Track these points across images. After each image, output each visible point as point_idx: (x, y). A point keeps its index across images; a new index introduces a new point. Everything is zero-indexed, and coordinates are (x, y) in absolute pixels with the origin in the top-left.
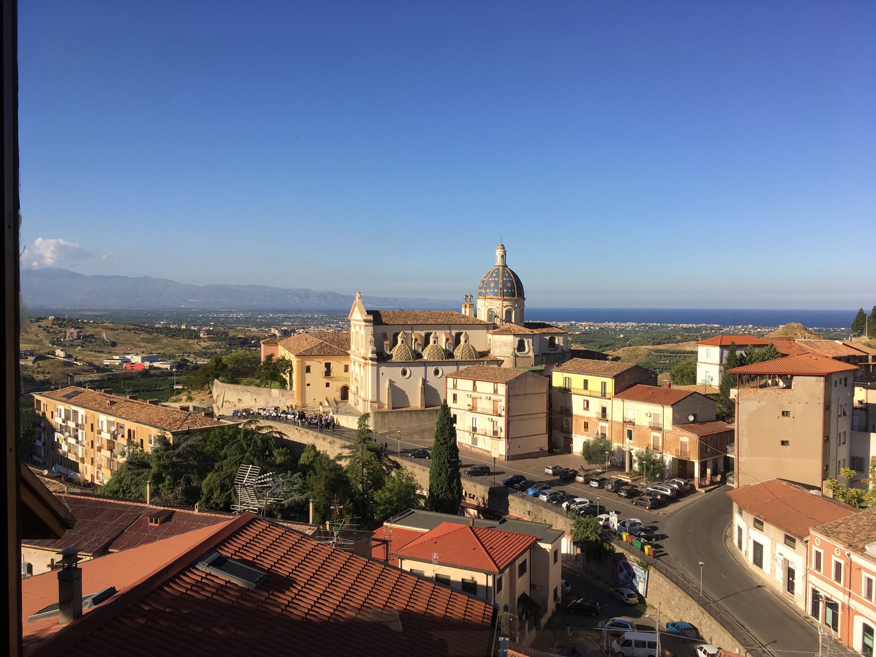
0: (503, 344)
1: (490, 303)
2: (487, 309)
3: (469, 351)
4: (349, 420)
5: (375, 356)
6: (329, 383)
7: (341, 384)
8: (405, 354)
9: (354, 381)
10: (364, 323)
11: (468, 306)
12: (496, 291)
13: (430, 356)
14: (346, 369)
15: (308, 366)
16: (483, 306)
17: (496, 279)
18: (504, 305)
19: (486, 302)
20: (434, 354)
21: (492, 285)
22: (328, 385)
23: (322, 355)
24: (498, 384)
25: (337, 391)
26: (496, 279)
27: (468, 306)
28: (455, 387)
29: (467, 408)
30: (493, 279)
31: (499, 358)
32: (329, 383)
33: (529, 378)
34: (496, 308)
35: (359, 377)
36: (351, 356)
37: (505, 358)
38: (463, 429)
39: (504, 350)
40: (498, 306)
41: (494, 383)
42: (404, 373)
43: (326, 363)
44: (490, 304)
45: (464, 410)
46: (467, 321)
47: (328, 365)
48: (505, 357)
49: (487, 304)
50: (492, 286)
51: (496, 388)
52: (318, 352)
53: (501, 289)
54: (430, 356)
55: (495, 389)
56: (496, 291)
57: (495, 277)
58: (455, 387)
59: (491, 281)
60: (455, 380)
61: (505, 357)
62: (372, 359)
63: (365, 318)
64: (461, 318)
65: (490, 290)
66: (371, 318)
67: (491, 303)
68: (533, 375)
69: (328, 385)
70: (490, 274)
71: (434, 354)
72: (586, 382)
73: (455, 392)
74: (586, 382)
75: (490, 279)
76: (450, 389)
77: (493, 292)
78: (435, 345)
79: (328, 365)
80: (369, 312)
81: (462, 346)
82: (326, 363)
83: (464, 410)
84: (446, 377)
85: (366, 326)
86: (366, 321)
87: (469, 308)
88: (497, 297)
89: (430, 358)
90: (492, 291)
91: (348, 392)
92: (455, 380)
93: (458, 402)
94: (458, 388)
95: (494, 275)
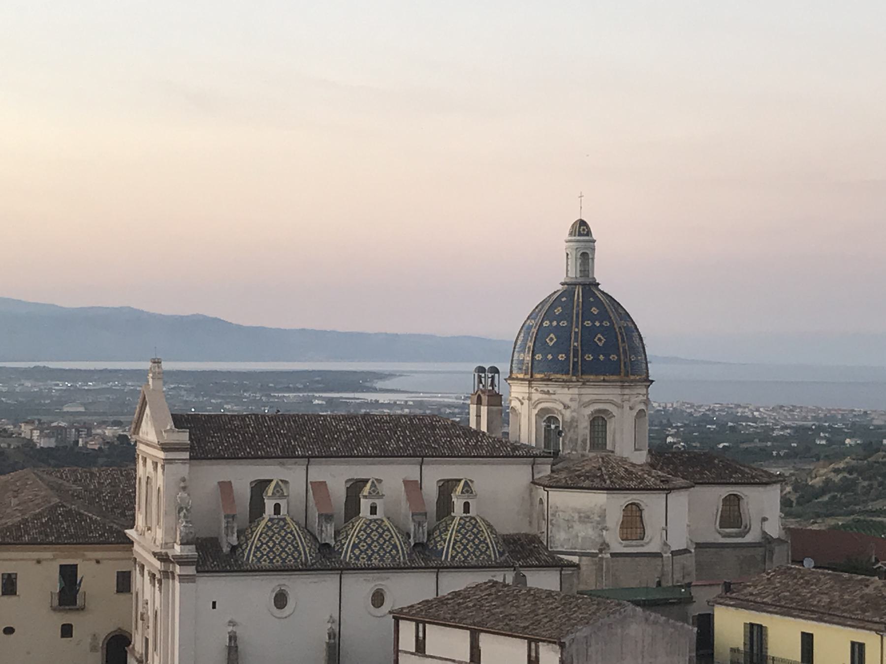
0: (576, 516)
1: (543, 392)
2: (535, 411)
3: (476, 535)
5: (191, 551)
6: (70, 626)
7: (105, 629)
8: (284, 544)
9: (140, 622)
10: (161, 455)
11: (485, 399)
12: (562, 357)
13: (357, 552)
14: (124, 583)
15: (9, 575)
16: (526, 402)
17: (564, 323)
18: (586, 399)
19: (533, 390)
20: (369, 546)
21: (551, 340)
22: (67, 631)
23: (51, 543)
24: (540, 643)
25: (94, 649)
26: (564, 323)
27: (485, 399)
30: (555, 323)
32: (70, 626)
33: (634, 626)
34: (561, 407)
35: (150, 614)
36: (136, 547)
37: (584, 558)
40: (568, 402)
41: (530, 641)
42: (281, 600)
43: (61, 566)
44: (547, 396)
46: (475, 446)
47: (69, 574)
48: (581, 555)
49: (536, 396)
50: (551, 344)
51: (533, 654)
52: (40, 533)
53: (576, 350)
54: (357, 552)
55: (533, 659)
56: (562, 357)
57: (559, 318)
59: (550, 330)
60: (421, 626)
61: (581, 555)
62: (182, 561)
63: (167, 438)
64: (458, 436)
66: (184, 437)
67: (548, 393)
68: (647, 620)
69: (67, 631)
70: (546, 308)
71: (369, 546)
72: (807, 640)
74: (807, 640)
75: (546, 324)
76: (406, 652)
77: (555, 359)
78: (375, 517)
79: (69, 574)
80: (180, 421)
81: (456, 521)
82: (61, 566)
84: (397, 620)
85: (167, 461)
86: (165, 447)
87: (489, 405)
88: (564, 377)
89: (357, 558)
90: (550, 357)
91: (126, 652)
92: (421, 626)
95: (558, 311)
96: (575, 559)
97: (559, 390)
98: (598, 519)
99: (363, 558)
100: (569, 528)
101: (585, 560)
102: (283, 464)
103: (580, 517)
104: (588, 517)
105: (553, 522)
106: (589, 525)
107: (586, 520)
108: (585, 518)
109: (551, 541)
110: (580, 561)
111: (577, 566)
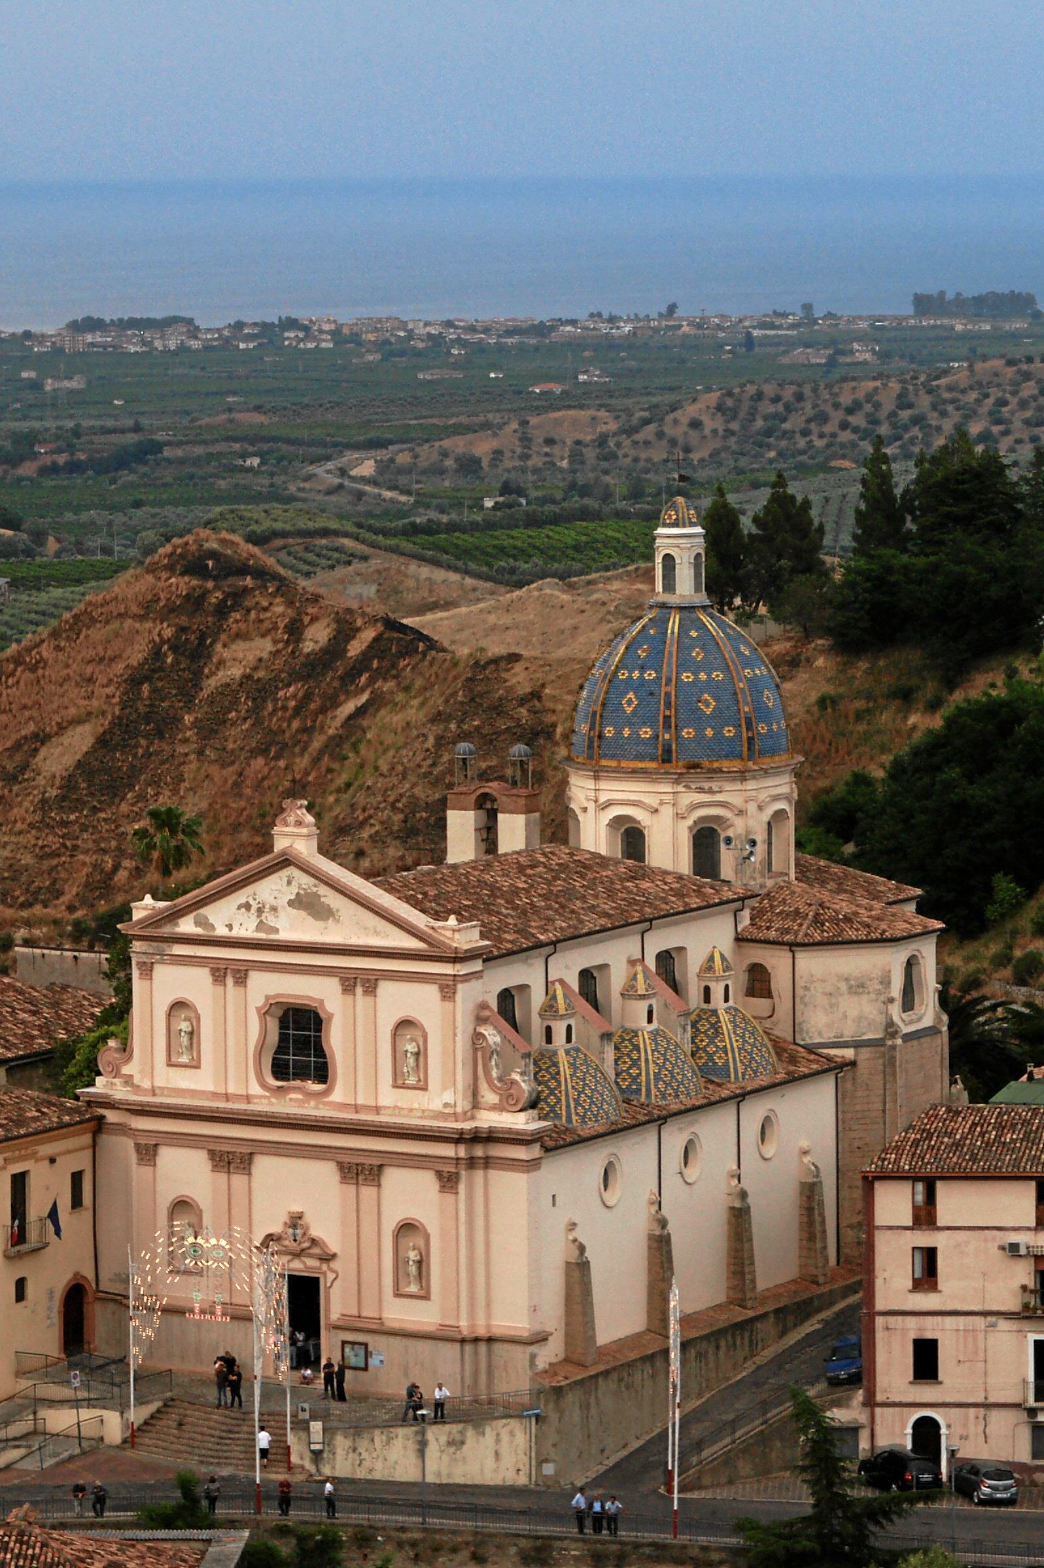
0: (843, 986)
1: (701, 790)
4: (432, 1450)
13: (661, 1085)
28: (925, 1216)
29: (1012, 1303)
30: (636, 674)
31: (832, 1052)
37: (864, 1050)
38: (980, 1399)
39: (853, 1013)
45: (985, 1314)
48: (857, 1045)
56: (729, 732)
58: (925, 1216)
59: (629, 683)
65: (700, 731)
73: (924, 1239)
76: (890, 1228)
83: (985, 1314)
90: (709, 732)
93: (941, 1285)
94: (939, 1224)
96: (849, 1053)
97: (728, 786)
98: (880, 987)
99: (670, 1095)
100: (832, 1006)
101: (865, 1054)
102: (525, 961)
103: (850, 987)
104: (862, 986)
105: (806, 999)
106: (865, 997)
107: (861, 990)
108: (858, 987)
109: (802, 1030)
110: (856, 1054)
111: (853, 1064)
